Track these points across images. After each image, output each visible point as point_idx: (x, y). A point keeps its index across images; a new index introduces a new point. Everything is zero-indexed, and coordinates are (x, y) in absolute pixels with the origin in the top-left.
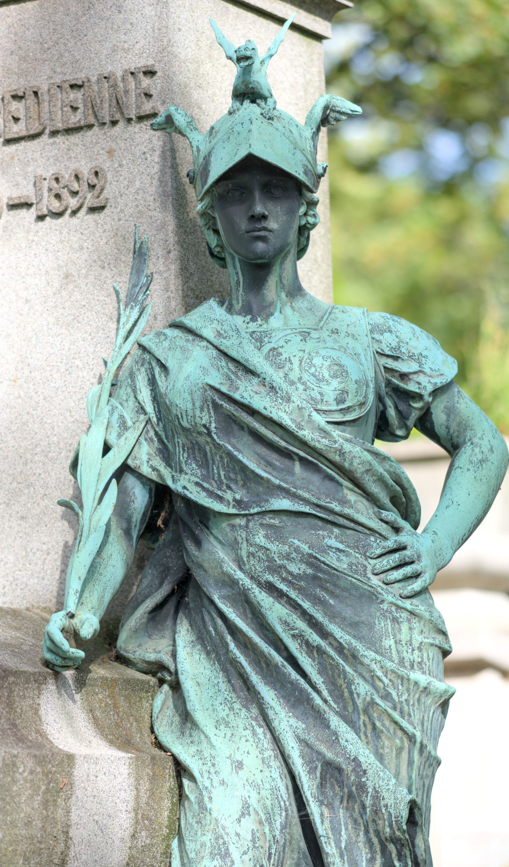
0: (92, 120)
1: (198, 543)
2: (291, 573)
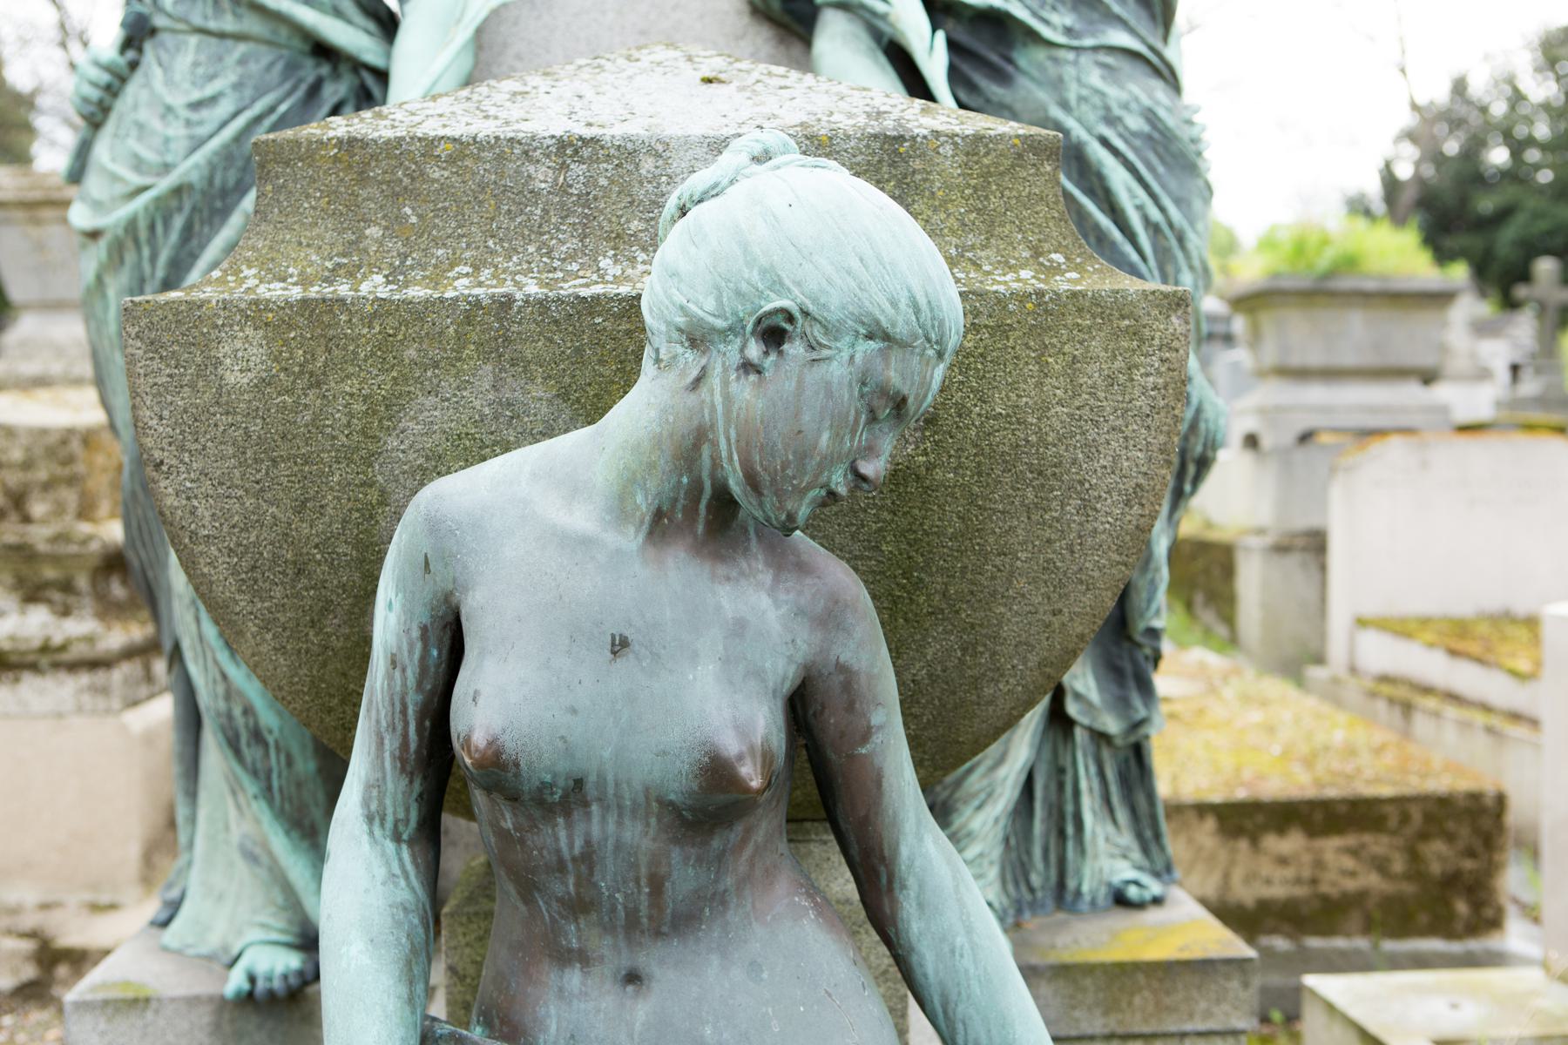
2: (1126, 128)
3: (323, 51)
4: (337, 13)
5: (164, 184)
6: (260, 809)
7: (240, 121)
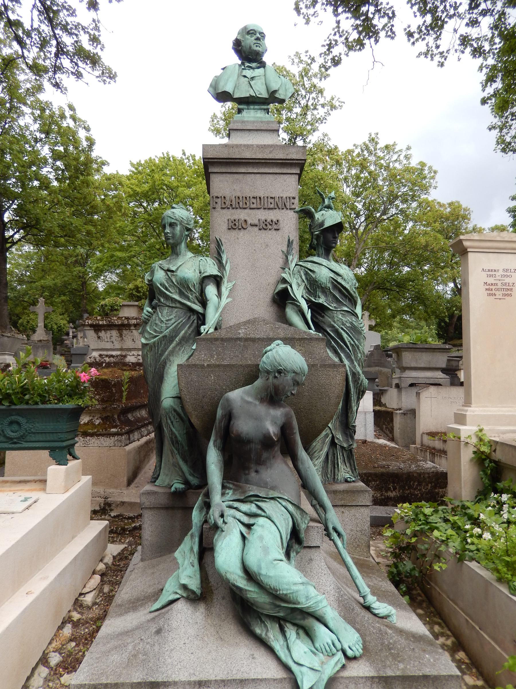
0: (276, 207)
1: (323, 317)
3: (191, 310)
4: (194, 303)
5: (161, 335)
6: (178, 457)
7: (176, 324)
